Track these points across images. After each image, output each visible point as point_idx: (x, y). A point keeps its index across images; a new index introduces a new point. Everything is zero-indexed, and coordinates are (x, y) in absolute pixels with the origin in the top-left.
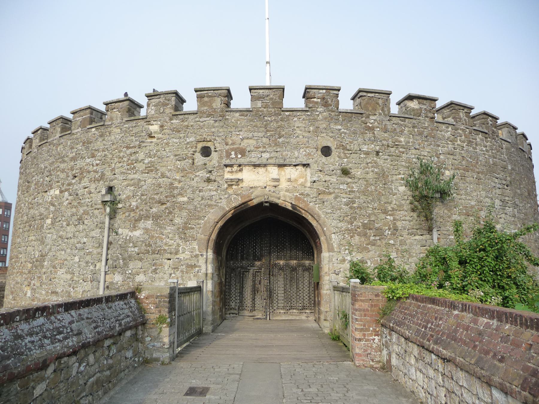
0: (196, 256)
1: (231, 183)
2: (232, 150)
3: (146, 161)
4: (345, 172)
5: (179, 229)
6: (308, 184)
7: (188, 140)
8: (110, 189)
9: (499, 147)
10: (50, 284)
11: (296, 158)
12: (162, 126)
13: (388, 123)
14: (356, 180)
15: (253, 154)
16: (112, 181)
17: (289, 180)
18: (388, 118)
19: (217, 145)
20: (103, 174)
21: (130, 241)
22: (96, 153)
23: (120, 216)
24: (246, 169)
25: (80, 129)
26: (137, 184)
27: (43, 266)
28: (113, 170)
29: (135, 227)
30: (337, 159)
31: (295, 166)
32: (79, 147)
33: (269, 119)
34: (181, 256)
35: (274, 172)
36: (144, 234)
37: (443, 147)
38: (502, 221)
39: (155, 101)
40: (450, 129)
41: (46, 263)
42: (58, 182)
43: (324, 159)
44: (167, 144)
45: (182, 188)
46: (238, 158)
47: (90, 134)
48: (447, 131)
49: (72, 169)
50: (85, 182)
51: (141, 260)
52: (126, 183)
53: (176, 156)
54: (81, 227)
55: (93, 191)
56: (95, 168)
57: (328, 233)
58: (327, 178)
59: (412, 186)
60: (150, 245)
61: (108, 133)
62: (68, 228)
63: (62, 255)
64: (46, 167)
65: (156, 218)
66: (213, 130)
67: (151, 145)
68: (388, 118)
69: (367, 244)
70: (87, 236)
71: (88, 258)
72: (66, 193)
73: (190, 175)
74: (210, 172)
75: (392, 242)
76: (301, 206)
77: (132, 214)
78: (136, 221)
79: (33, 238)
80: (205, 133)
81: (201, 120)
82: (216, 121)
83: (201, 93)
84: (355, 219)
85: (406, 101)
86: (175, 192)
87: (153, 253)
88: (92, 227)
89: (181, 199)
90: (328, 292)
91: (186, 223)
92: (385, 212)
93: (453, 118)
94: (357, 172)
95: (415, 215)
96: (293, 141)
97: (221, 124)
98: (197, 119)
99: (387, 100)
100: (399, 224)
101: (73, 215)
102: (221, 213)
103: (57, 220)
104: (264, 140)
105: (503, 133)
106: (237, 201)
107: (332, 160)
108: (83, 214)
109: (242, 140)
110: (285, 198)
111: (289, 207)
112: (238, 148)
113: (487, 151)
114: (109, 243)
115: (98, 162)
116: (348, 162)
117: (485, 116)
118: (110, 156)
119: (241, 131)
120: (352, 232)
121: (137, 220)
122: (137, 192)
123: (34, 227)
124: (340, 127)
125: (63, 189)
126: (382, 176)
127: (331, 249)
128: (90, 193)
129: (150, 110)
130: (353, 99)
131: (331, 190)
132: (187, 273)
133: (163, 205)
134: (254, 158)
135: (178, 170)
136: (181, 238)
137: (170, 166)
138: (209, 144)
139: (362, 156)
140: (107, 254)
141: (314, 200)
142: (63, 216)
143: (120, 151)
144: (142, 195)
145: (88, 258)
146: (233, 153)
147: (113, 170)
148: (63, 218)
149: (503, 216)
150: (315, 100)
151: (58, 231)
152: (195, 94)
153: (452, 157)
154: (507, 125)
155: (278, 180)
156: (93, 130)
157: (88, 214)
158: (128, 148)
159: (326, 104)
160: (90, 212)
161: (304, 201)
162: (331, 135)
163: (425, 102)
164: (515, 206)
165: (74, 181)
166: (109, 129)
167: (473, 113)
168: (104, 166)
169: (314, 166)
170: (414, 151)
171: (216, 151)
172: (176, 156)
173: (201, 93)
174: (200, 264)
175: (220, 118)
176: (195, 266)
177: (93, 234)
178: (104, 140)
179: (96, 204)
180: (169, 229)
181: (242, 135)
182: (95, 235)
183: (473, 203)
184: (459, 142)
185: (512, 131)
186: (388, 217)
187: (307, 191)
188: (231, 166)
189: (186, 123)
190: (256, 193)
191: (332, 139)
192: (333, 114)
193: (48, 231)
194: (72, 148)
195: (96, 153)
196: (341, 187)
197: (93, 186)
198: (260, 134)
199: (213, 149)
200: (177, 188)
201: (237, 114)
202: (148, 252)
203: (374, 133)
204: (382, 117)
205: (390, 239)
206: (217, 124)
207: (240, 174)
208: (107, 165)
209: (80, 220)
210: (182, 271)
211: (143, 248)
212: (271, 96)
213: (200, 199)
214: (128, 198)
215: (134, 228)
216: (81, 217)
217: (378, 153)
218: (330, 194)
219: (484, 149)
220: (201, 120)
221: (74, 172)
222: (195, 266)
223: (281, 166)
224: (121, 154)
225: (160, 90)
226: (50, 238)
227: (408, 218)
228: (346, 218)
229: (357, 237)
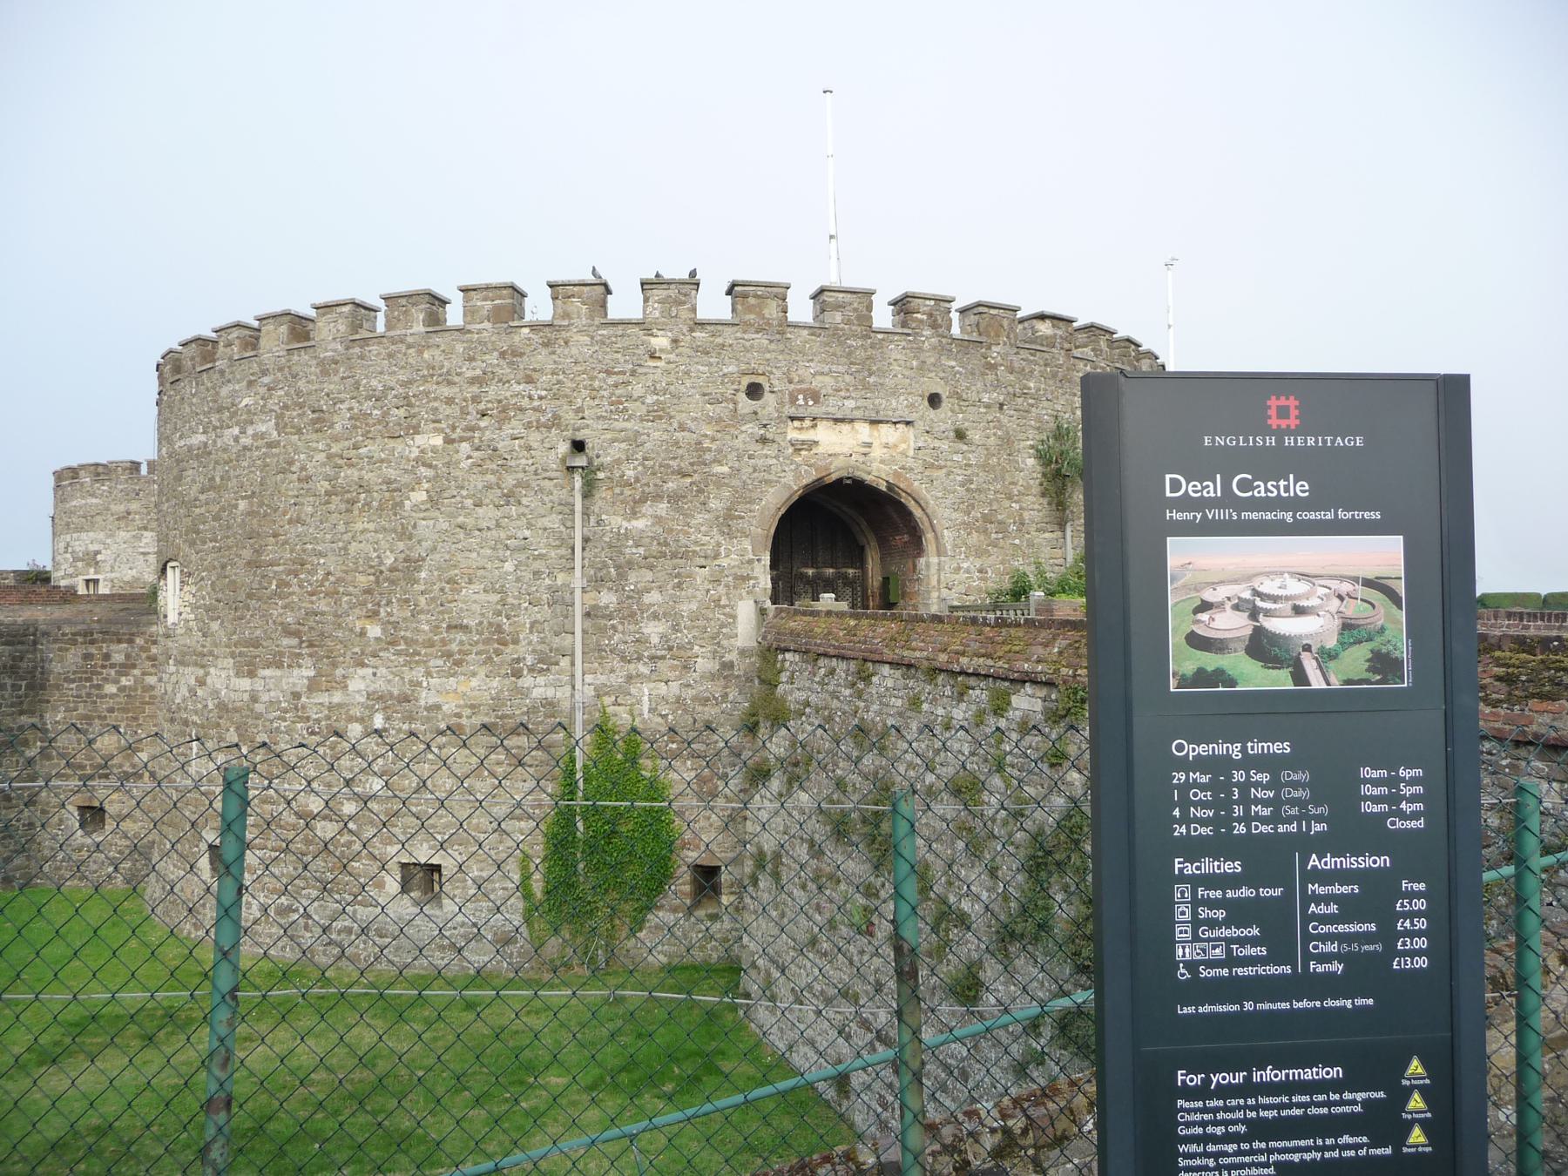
0: (750, 562)
1: (798, 447)
2: (800, 391)
5: (717, 518)
6: (911, 453)
8: (579, 446)
11: (894, 410)
12: (675, 341)
15: (831, 400)
17: (886, 446)
19: (775, 382)
20: (556, 417)
21: (627, 535)
23: (602, 494)
24: (822, 425)
25: (487, 325)
26: (634, 440)
28: (580, 410)
29: (634, 513)
32: (493, 358)
34: (724, 562)
35: (864, 430)
36: (653, 525)
39: (658, 293)
41: (423, 575)
43: (932, 413)
44: (687, 373)
45: (719, 451)
46: (807, 405)
49: (476, 399)
50: (515, 426)
51: (651, 568)
52: (609, 436)
55: (535, 445)
57: (938, 529)
58: (937, 444)
59: (1043, 457)
60: (666, 544)
62: (480, 511)
65: (675, 498)
66: (768, 356)
70: (530, 526)
71: (537, 565)
73: (732, 430)
77: (627, 492)
86: (708, 456)
87: (674, 556)
89: (718, 469)
91: (729, 509)
92: (1010, 497)
94: (975, 435)
95: (1045, 501)
96: (889, 382)
97: (781, 347)
100: (1026, 515)
102: (787, 495)
104: (848, 378)
109: (814, 375)
110: (877, 473)
114: (586, 540)
115: (544, 393)
116: (965, 419)
121: (643, 500)
125: (454, 436)
126: (1007, 442)
128: (529, 449)
131: (942, 463)
133: (684, 481)
134: (832, 406)
135: (709, 420)
137: (693, 409)
138: (760, 380)
143: (592, 379)
144: (645, 459)
145: (537, 565)
147: (580, 410)
155: (869, 445)
156: (526, 330)
157: (528, 486)
158: (609, 373)
160: (534, 484)
163: (1061, 324)
169: (920, 425)
170: (1045, 404)
176: (748, 578)
177: (545, 522)
180: (699, 518)
181: (814, 367)
182: (550, 525)
187: (910, 463)
188: (801, 419)
189: (719, 340)
195: (535, 375)
197: (534, 438)
199: (767, 388)
200: (709, 450)
201: (805, 332)
202: (664, 555)
204: (1007, 348)
206: (772, 347)
207: (812, 432)
208: (563, 401)
210: (727, 586)
214: (618, 462)
215: (634, 514)
216: (511, 491)
221: (482, 406)
222: (748, 578)
225: (667, 275)
229: (975, 535)
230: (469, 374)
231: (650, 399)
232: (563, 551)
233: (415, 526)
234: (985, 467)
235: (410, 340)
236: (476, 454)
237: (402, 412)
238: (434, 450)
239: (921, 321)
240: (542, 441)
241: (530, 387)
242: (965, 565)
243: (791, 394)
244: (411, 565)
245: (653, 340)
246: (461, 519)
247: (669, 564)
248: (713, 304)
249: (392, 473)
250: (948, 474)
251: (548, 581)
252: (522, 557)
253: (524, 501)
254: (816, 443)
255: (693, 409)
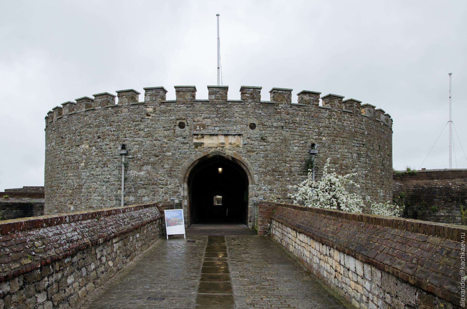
0: (178, 186)
1: (197, 145)
2: (198, 125)
3: (146, 130)
4: (263, 139)
6: (241, 146)
7: (171, 118)
8: (124, 147)
9: (360, 120)
10: (87, 203)
11: (235, 130)
12: (154, 109)
13: (290, 109)
14: (269, 144)
15: (210, 127)
16: (124, 141)
17: (230, 144)
18: (290, 106)
20: (118, 137)
21: (138, 177)
22: (112, 123)
25: (100, 107)
26: (141, 144)
27: (81, 192)
28: (125, 135)
30: (259, 131)
31: (234, 135)
32: (101, 118)
33: (219, 106)
34: (169, 187)
35: (222, 139)
37: (322, 123)
38: (357, 166)
40: (328, 111)
41: (83, 190)
42: (87, 140)
43: (251, 131)
44: (158, 120)
47: (108, 111)
48: (326, 113)
51: (145, 188)
52: (133, 143)
53: (164, 127)
54: (106, 169)
55: (112, 147)
56: (113, 133)
57: (252, 174)
58: (253, 142)
61: (120, 111)
62: (97, 169)
63: (94, 185)
64: (76, 130)
65: (153, 164)
66: (186, 112)
67: (148, 120)
68: (290, 106)
69: (275, 180)
72: (94, 147)
74: (185, 138)
75: (288, 179)
76: (237, 158)
78: (141, 166)
79: (72, 174)
80: (181, 114)
81: (179, 106)
82: (187, 107)
83: (179, 90)
84: (268, 166)
85: (301, 95)
86: (165, 149)
87: (153, 184)
88: (113, 169)
90: (252, 206)
91: (171, 168)
92: (285, 162)
93: (330, 105)
94: (270, 139)
96: (234, 120)
97: (191, 109)
98: (176, 106)
99: (290, 95)
100: (293, 169)
101: (99, 161)
102: (192, 162)
103: (89, 164)
104: (216, 119)
105: (364, 112)
106: (200, 155)
107: (256, 132)
108: (107, 161)
109: (203, 119)
111: (230, 159)
112: (201, 124)
113: (351, 124)
114: (126, 179)
115: (115, 129)
117: (352, 102)
118: (122, 126)
119: (202, 113)
120: (265, 174)
122: (141, 148)
123: (71, 167)
124: (261, 112)
125: (91, 145)
127: (253, 183)
128: (110, 148)
129: (146, 98)
130: (271, 92)
131: (255, 150)
132: (173, 196)
133: (158, 157)
134: (210, 130)
136: (168, 176)
138: (184, 121)
139: (273, 129)
140: (125, 185)
141: (245, 155)
142: (93, 162)
144: (144, 151)
145: (112, 187)
146: (198, 127)
147: (125, 135)
148: (93, 163)
149: (358, 163)
150: (247, 95)
151: (90, 171)
152: (175, 90)
153: (327, 129)
154: (367, 106)
155: (223, 144)
156: (110, 108)
158: (134, 121)
159: (253, 98)
160: (112, 160)
161: (239, 156)
162: (256, 116)
163: (313, 95)
164: (367, 156)
165: (99, 140)
166: (120, 109)
167: (344, 100)
168: (119, 132)
170: (304, 126)
171: (188, 126)
172: (164, 127)
173: (179, 90)
174: (180, 191)
175: (190, 105)
176: (177, 192)
177: (114, 173)
178: (117, 116)
179: (115, 155)
183: (339, 156)
184: (333, 120)
185: (372, 110)
186: (287, 165)
187: (241, 150)
189: (169, 108)
190: (212, 150)
191: (256, 119)
192: (257, 103)
193: (83, 171)
194: (96, 119)
196: (261, 147)
197: (112, 144)
198: (214, 116)
199: (186, 124)
201: (201, 103)
203: (281, 115)
204: (287, 105)
205: (287, 177)
206: (188, 109)
207: (202, 139)
208: (120, 132)
209: (105, 165)
211: (146, 181)
212: (221, 92)
213: (179, 154)
214: (136, 152)
215: (140, 170)
217: (282, 127)
218: (254, 151)
219: (349, 123)
220: (179, 106)
221: (98, 135)
222: (177, 192)
223: (226, 135)
224: (130, 125)
226: (84, 175)
227: (298, 165)
228: (262, 166)
229: (268, 176)
230: (95, 124)
231: (146, 130)
232: (119, 183)
233: (81, 175)
234: (275, 151)
235: (82, 113)
236: (97, 150)
237: (79, 137)
238: (86, 149)
239: (248, 97)
240: (114, 146)
241: (111, 127)
242: (264, 188)
243: (194, 126)
244: (81, 186)
245: (147, 109)
246: (92, 172)
247: (151, 187)
248: (171, 96)
249: (77, 157)
250: (257, 154)
251: (115, 193)
252: (108, 184)
253: (109, 166)
254: (203, 143)
255: (161, 133)
